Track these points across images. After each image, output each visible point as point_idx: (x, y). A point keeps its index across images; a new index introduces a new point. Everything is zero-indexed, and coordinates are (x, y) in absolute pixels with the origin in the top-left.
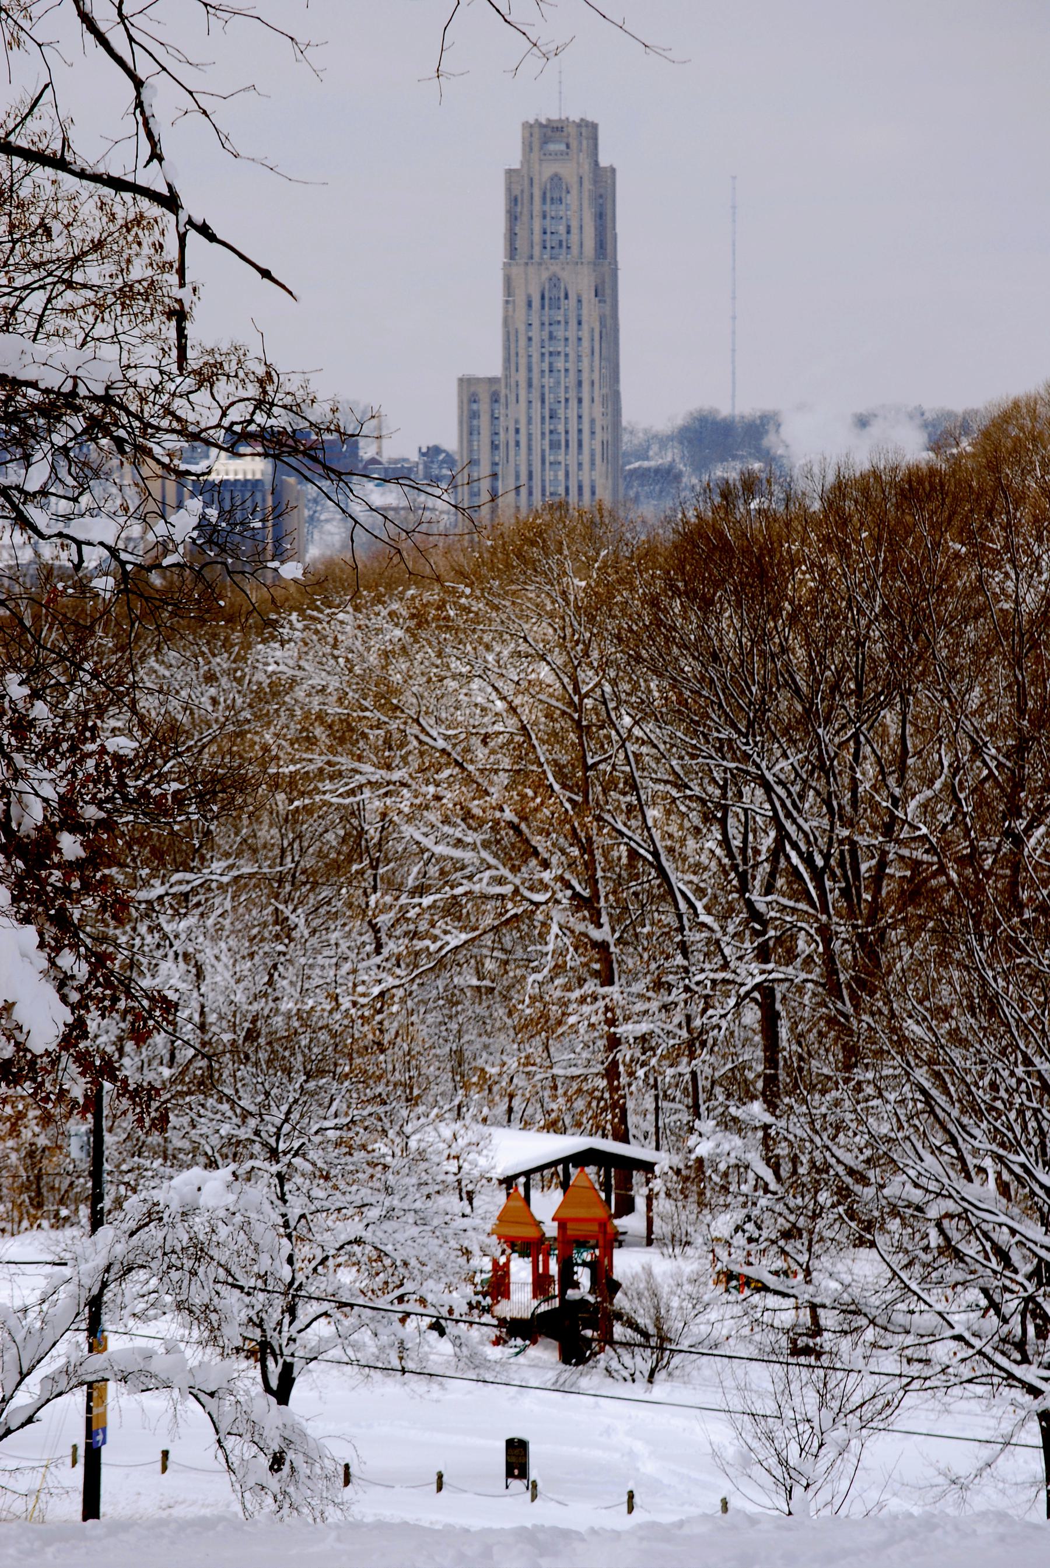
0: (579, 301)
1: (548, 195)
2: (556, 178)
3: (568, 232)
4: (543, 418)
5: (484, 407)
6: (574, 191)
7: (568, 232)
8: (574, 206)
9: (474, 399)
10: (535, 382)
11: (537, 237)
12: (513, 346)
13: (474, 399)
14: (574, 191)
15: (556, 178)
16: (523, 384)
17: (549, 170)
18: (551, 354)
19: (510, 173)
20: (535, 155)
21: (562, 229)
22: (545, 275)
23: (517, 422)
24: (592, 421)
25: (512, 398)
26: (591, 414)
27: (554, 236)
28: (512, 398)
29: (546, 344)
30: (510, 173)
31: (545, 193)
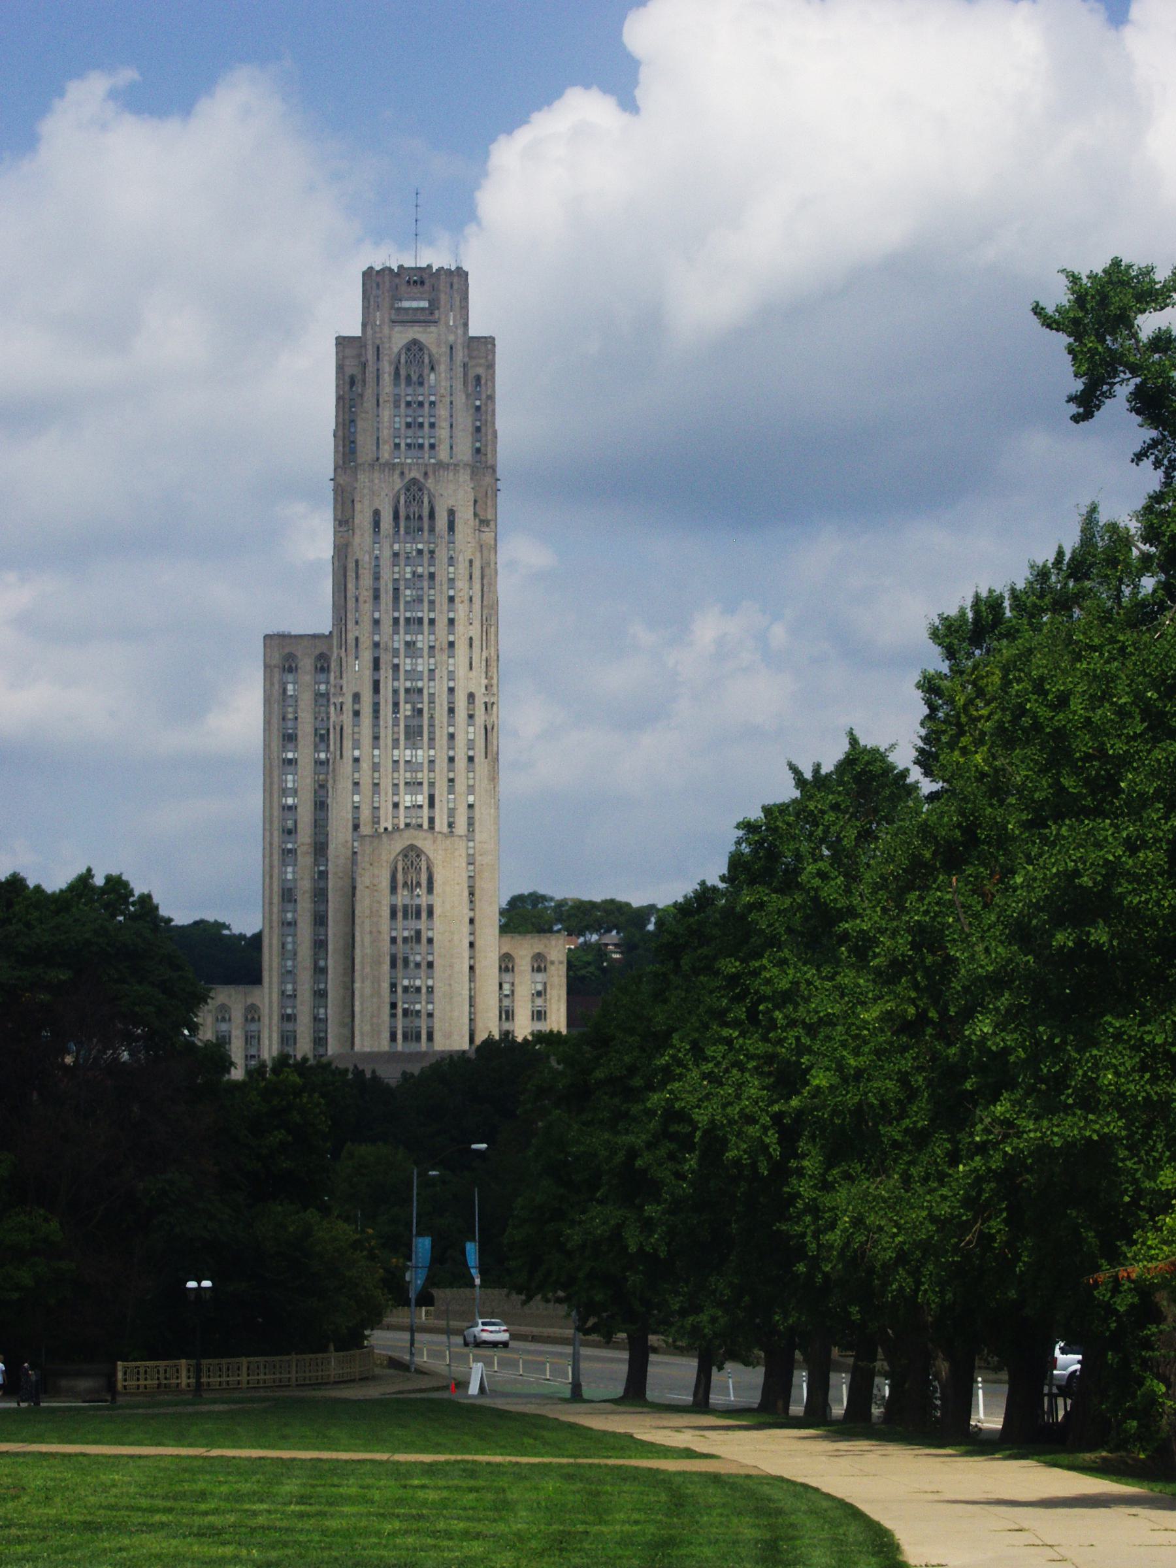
1: (403, 372)
2: (415, 347)
6: (442, 368)
9: (289, 666)
12: (351, 586)
15: (415, 347)
19: (343, 343)
22: (398, 484)
23: (357, 697)
24: (471, 696)
30: (343, 343)
31: (397, 370)
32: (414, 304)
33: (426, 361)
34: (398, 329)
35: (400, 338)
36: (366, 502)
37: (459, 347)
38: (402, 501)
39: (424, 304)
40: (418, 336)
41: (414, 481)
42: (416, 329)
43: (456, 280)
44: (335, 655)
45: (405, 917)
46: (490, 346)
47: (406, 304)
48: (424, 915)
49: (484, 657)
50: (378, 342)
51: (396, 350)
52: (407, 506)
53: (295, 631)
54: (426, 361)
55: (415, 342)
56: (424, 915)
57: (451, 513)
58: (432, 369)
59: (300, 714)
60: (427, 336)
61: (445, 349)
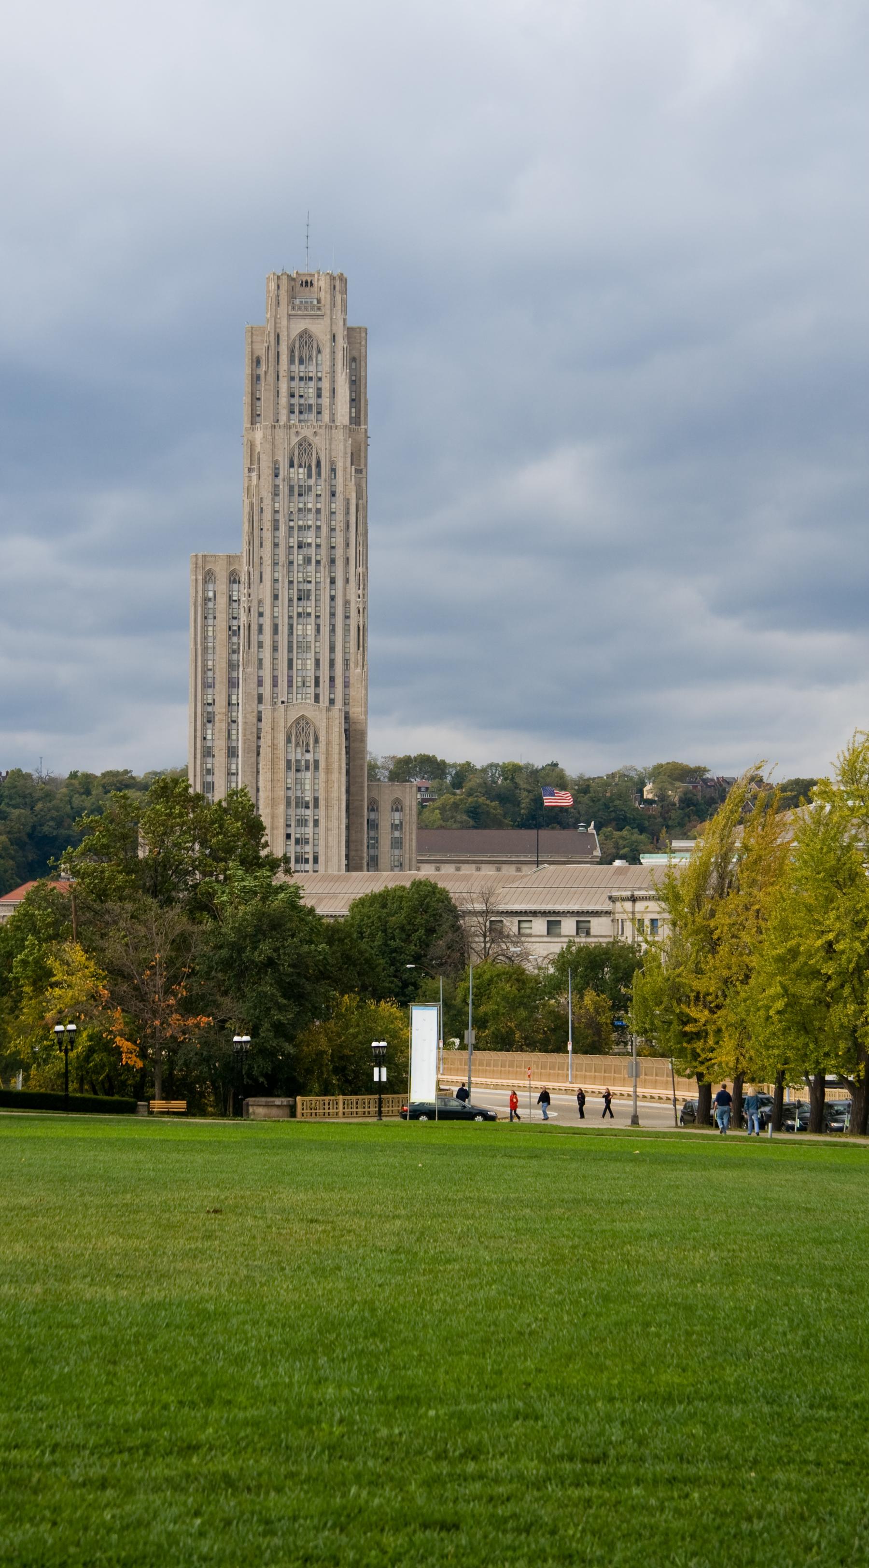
0: (333, 470)
1: (297, 353)
3: (319, 396)
4: (290, 600)
5: (221, 585)
6: (326, 351)
7: (319, 396)
8: (326, 367)
10: (282, 559)
11: (284, 400)
13: (209, 577)
14: (326, 351)
16: (267, 560)
17: (299, 326)
18: (300, 528)
20: (284, 309)
21: (312, 392)
22: (295, 440)
23: (260, 602)
24: (347, 603)
25: (255, 577)
26: (345, 595)
27: (302, 401)
28: (255, 577)
29: (295, 517)
33: (315, 346)
38: (296, 453)
41: (305, 439)
43: (338, 283)
45: (297, 806)
48: (312, 767)
51: (292, 337)
52: (299, 458)
54: (315, 346)
55: (305, 331)
56: (312, 767)
57: (332, 463)
59: (217, 615)
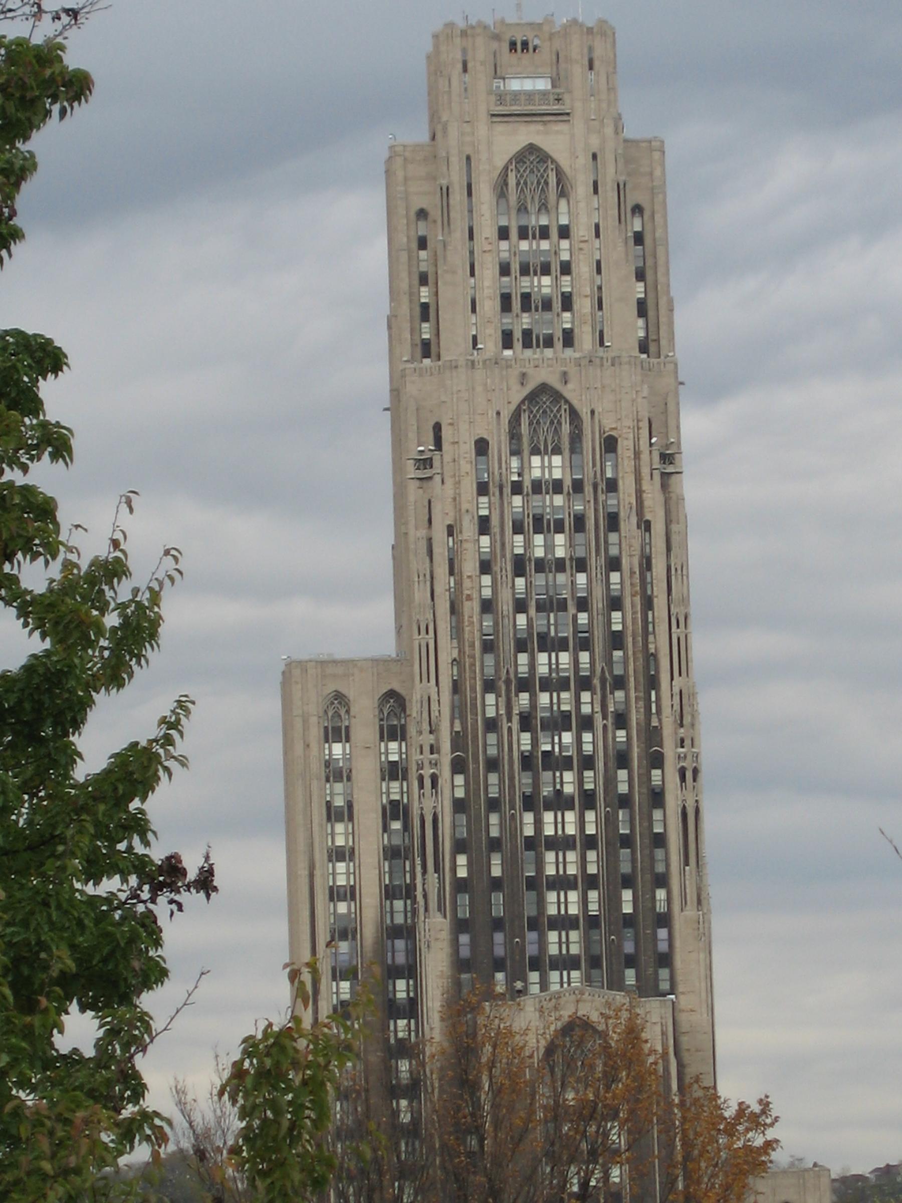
2: (532, 157)
15: (532, 157)
32: (528, 85)
34: (500, 128)
35: (511, 140)
36: (464, 427)
37: (609, 157)
39: (542, 85)
40: (538, 141)
42: (533, 128)
44: (416, 697)
46: (656, 155)
47: (515, 85)
49: (676, 690)
50: (468, 150)
53: (341, 654)
54: (552, 179)
55: (532, 148)
58: (563, 193)
60: (554, 141)
61: (583, 160)
